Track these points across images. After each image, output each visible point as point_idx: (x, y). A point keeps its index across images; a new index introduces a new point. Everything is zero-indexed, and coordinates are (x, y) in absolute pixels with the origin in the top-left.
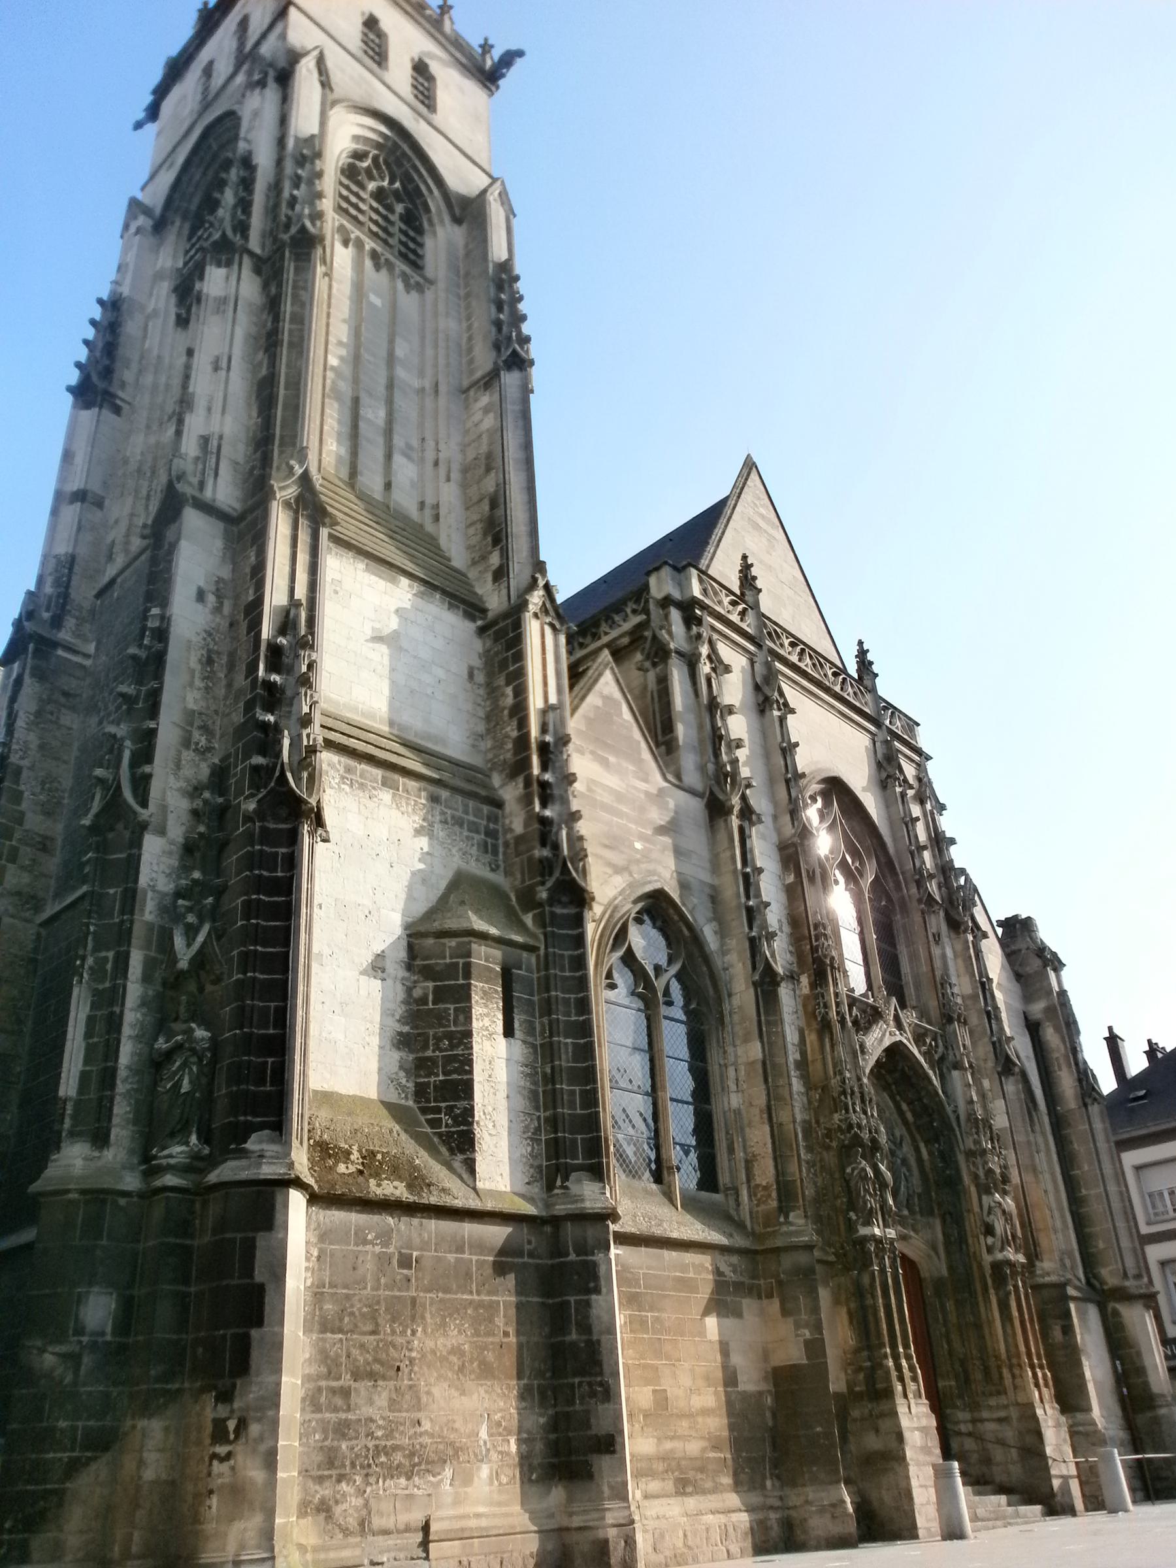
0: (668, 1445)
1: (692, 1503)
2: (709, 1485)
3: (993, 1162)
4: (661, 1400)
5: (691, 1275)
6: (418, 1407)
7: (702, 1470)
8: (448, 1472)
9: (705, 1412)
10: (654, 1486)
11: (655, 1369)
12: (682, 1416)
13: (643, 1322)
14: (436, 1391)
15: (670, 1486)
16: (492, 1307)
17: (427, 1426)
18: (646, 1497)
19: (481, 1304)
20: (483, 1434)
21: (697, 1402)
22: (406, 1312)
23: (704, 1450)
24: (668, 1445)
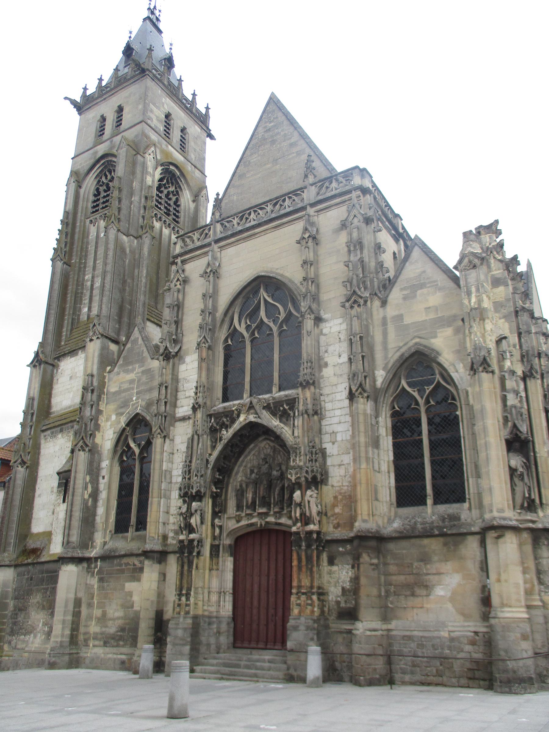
0: (104, 629)
1: (107, 649)
2: (115, 644)
3: (291, 474)
4: (104, 614)
5: (124, 567)
6: (29, 618)
7: (113, 638)
8: (32, 635)
9: (118, 618)
10: (97, 643)
11: (104, 603)
12: (110, 619)
13: (103, 587)
14: (33, 613)
15: (102, 643)
16: (47, 589)
17: (30, 623)
18: (94, 646)
19: (44, 589)
20: (41, 625)
21: (117, 614)
22: (29, 592)
23: (117, 632)
24: (104, 629)
